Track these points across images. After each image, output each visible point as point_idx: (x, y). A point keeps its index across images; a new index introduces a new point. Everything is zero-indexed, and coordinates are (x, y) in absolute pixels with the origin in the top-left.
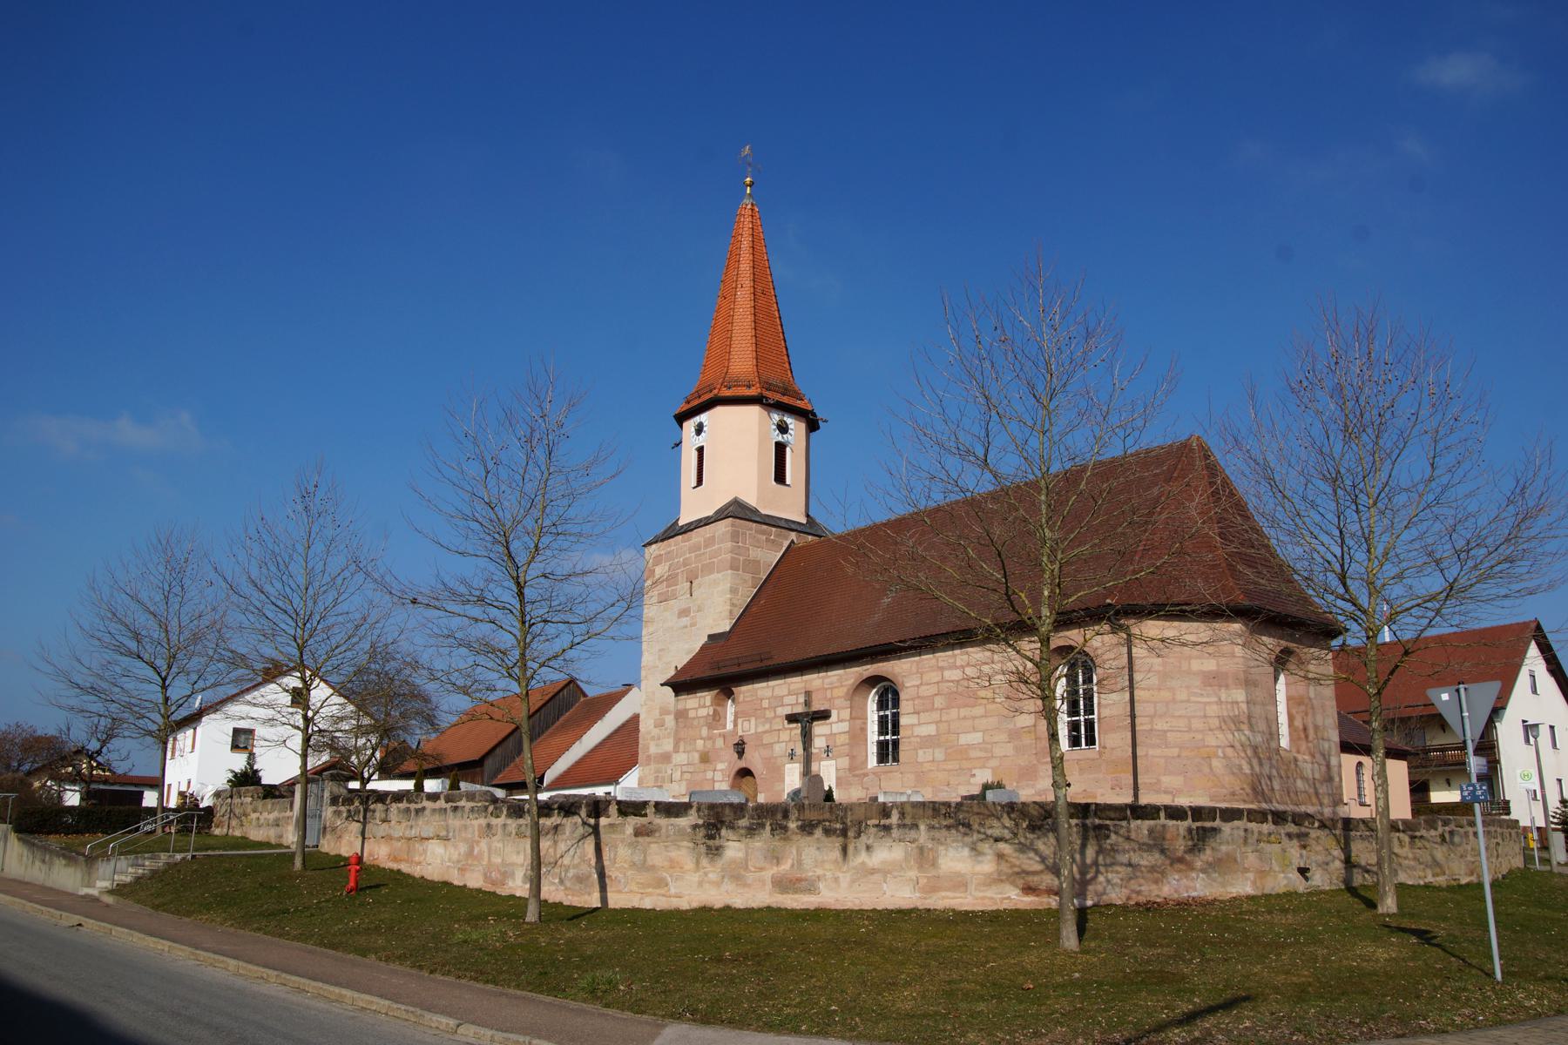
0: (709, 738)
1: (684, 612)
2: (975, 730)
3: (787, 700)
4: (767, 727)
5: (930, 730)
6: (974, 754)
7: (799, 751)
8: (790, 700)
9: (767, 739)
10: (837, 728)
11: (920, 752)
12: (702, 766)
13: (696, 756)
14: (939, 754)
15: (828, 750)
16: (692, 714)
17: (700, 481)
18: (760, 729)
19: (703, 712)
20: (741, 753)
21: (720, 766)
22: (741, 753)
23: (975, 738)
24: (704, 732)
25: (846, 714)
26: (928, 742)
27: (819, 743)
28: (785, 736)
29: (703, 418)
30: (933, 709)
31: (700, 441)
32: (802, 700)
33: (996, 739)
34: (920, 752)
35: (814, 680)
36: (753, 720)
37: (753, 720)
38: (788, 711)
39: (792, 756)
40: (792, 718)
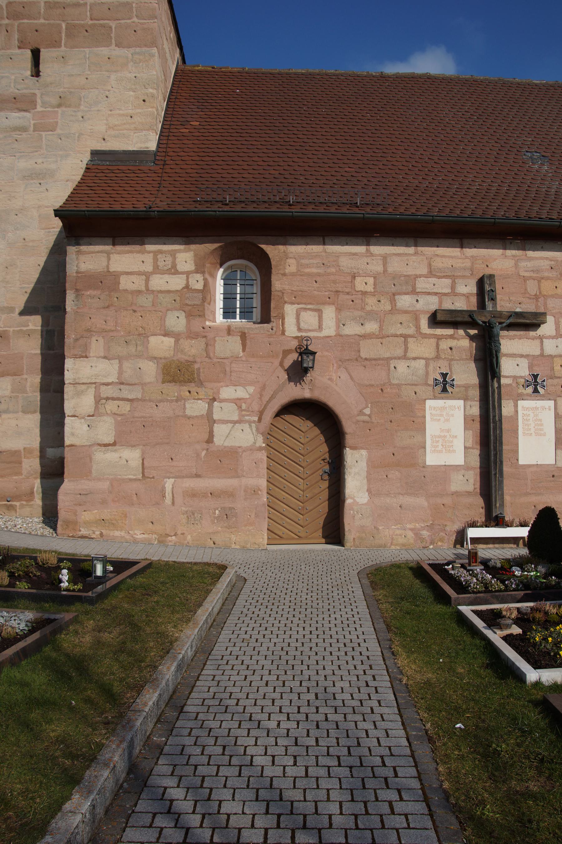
0: (192, 335)
4: (371, 327)
7: (467, 375)
8: (444, 285)
12: (173, 390)
13: (150, 370)
16: (125, 283)
18: (352, 329)
19: (177, 283)
20: (298, 371)
21: (227, 392)
22: (298, 371)
24: (177, 321)
32: (469, 288)
35: (499, 260)
36: (329, 313)
37: (329, 313)
38: (433, 304)
39: (444, 386)
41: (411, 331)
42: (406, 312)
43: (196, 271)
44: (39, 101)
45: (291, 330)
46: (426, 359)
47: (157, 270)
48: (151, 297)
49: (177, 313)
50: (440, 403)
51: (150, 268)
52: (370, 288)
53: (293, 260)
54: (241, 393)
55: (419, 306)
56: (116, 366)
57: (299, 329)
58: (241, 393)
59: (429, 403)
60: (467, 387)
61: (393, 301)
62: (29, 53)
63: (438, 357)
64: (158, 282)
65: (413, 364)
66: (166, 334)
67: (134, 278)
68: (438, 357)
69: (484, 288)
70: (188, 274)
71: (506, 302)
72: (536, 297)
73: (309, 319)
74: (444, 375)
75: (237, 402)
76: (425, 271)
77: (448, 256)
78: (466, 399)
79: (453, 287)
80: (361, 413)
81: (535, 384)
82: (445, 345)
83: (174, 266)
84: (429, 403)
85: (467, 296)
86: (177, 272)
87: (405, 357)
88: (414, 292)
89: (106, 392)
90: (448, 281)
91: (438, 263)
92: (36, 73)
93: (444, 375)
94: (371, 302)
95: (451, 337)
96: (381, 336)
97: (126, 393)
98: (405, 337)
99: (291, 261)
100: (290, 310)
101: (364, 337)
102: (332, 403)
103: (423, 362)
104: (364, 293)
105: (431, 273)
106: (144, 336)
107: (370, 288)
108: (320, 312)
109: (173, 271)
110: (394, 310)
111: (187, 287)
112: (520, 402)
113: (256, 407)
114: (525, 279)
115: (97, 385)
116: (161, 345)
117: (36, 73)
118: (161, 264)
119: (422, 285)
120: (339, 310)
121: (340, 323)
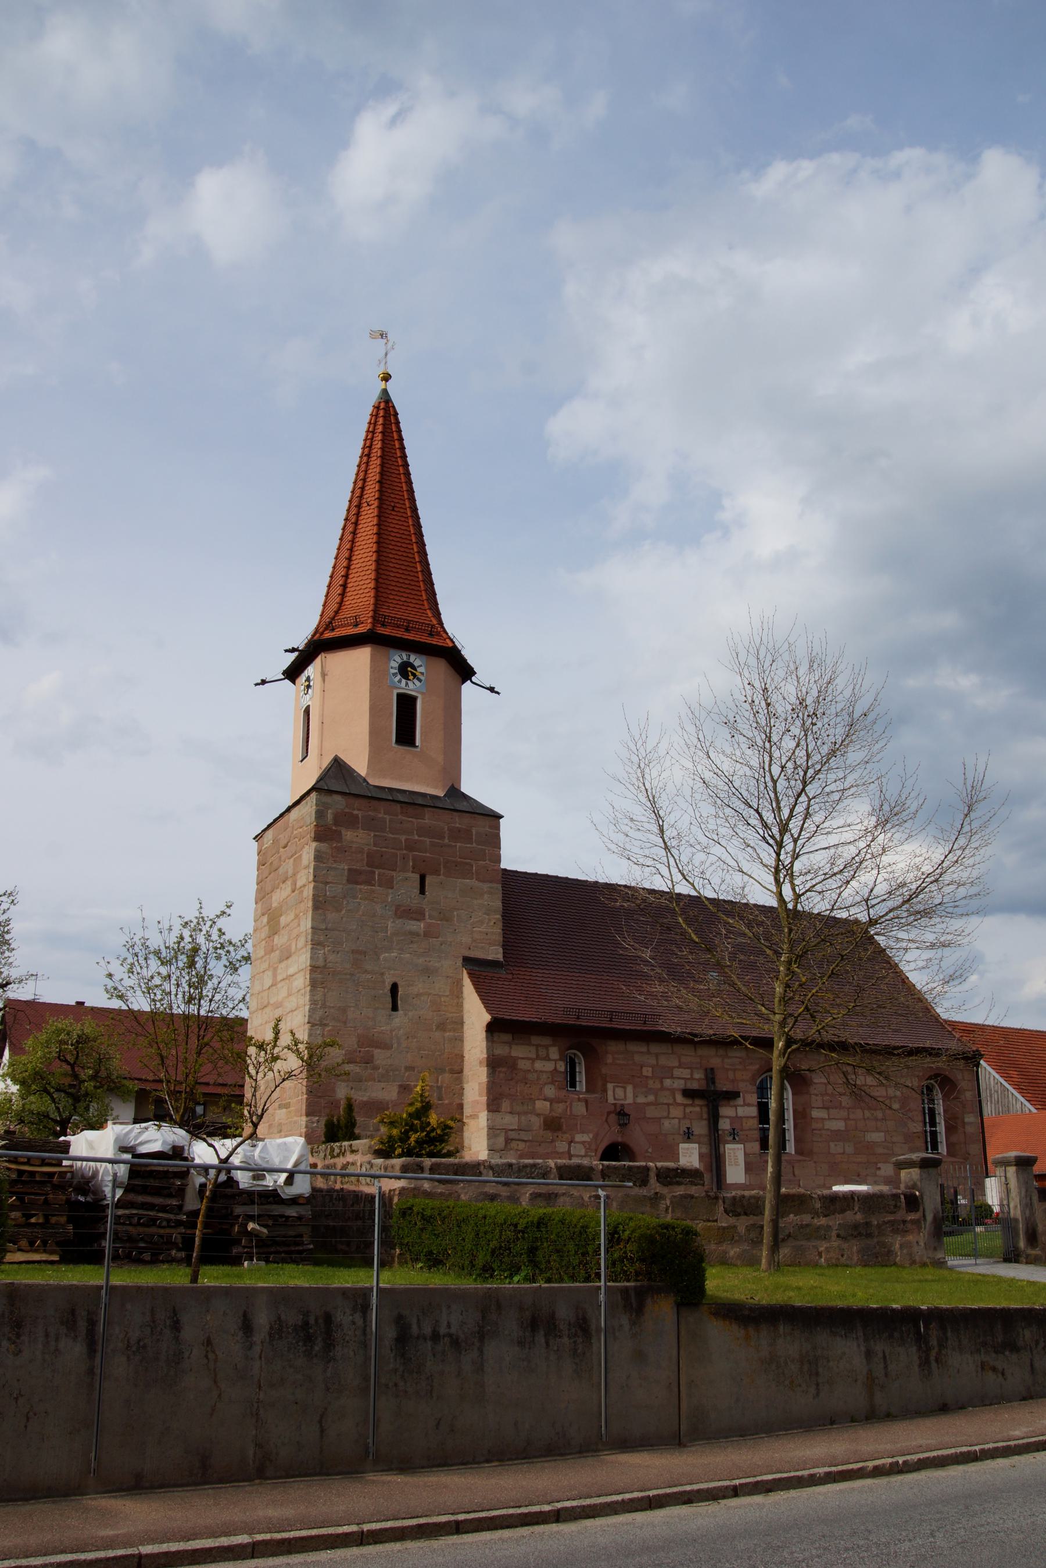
1: (418, 915)
2: (878, 1130)
3: (677, 1072)
4: (651, 1098)
5: (840, 1125)
6: (880, 1150)
7: (700, 1128)
8: (686, 1073)
9: (651, 1112)
10: (742, 1111)
11: (832, 1145)
12: (549, 1135)
13: (536, 1122)
14: (850, 1149)
15: (733, 1133)
16: (523, 1065)
17: (307, 711)
18: (641, 1100)
21: (579, 1138)
23: (876, 1137)
24: (550, 1091)
25: (753, 1099)
26: (838, 1136)
27: (724, 1125)
28: (677, 1112)
29: (416, 660)
30: (840, 1107)
31: (411, 687)
32: (699, 1075)
33: (894, 1139)
34: (832, 1145)
35: (714, 1058)
36: (630, 1088)
37: (630, 1088)
38: (679, 1084)
39: (688, 1136)
40: (688, 1093)
41: (671, 1101)
42: (669, 1089)
43: (560, 1059)
44: (427, 914)
45: (611, 1100)
46: (679, 1119)
47: (538, 1057)
48: (535, 1075)
49: (550, 1086)
50: (686, 1145)
51: (534, 1056)
52: (650, 1074)
53: (614, 1053)
54: (586, 1138)
55: (675, 1085)
56: (516, 1118)
57: (615, 1099)
58: (586, 1138)
59: (681, 1145)
60: (700, 1136)
61: (662, 1082)
62: (417, 876)
63: (685, 1118)
64: (539, 1065)
65: (673, 1121)
66: (545, 1100)
67: (524, 1062)
68: (685, 1118)
69: (710, 1075)
70: (555, 1061)
71: (723, 1085)
72: (733, 1081)
73: (620, 1092)
74: (688, 1128)
75: (583, 1143)
76: (677, 1064)
77: (688, 1054)
78: (699, 1143)
79: (692, 1074)
80: (647, 1151)
81: (733, 1133)
82: (688, 1110)
83: (548, 1055)
84: (681, 1145)
85: (699, 1080)
86: (549, 1060)
87: (668, 1117)
88: (672, 1077)
89: (512, 1135)
90: (689, 1071)
91: (684, 1059)
92: (422, 891)
93: (688, 1128)
94: (651, 1082)
95: (691, 1105)
96: (655, 1104)
97: (523, 1136)
98: (668, 1105)
99: (610, 1056)
100: (610, 1086)
101: (648, 1104)
102: (631, 1145)
103: (677, 1121)
104: (647, 1077)
105: (680, 1067)
106: (532, 1101)
107: (650, 1074)
108: (625, 1088)
109: (547, 1058)
110: (663, 1088)
111: (555, 1069)
112: (727, 1146)
113: (593, 1147)
114: (728, 1070)
115: (507, 1131)
116: (542, 1106)
117: (422, 891)
118: (540, 1053)
119: (677, 1072)
120: (634, 1087)
121: (635, 1096)
